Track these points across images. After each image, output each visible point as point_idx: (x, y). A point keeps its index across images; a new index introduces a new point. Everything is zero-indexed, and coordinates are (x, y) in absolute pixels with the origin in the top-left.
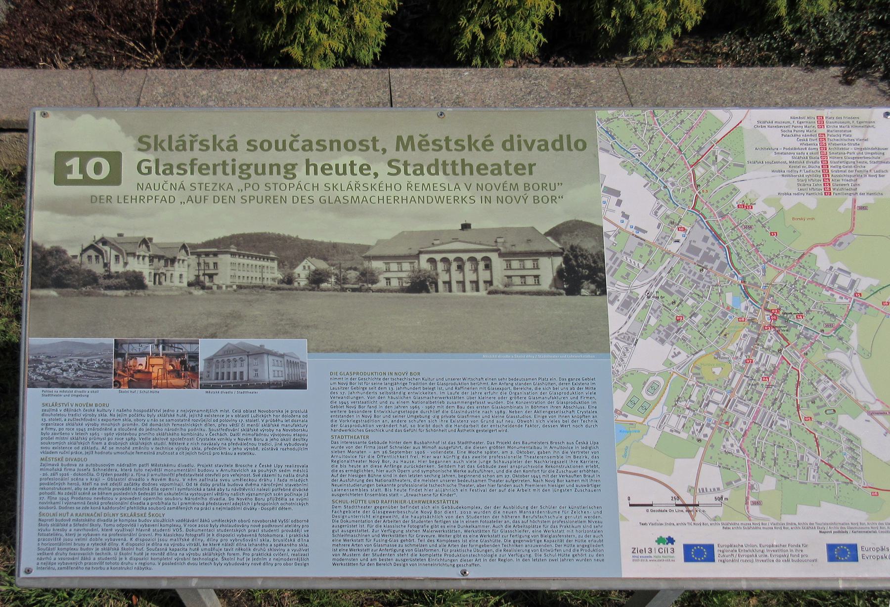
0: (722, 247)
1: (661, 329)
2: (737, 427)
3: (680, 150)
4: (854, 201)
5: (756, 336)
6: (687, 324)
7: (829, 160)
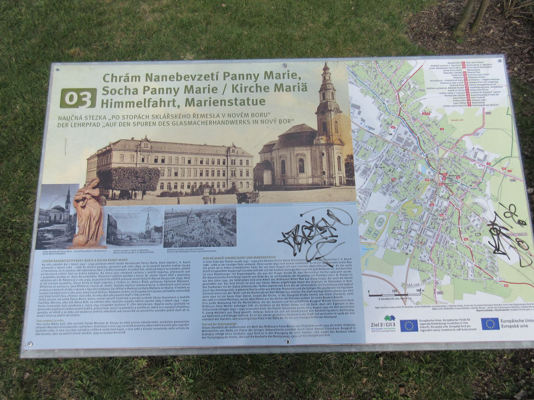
0: (415, 137)
1: (384, 186)
2: (427, 245)
3: (391, 82)
4: (484, 109)
5: (435, 189)
6: (398, 183)
7: (469, 86)
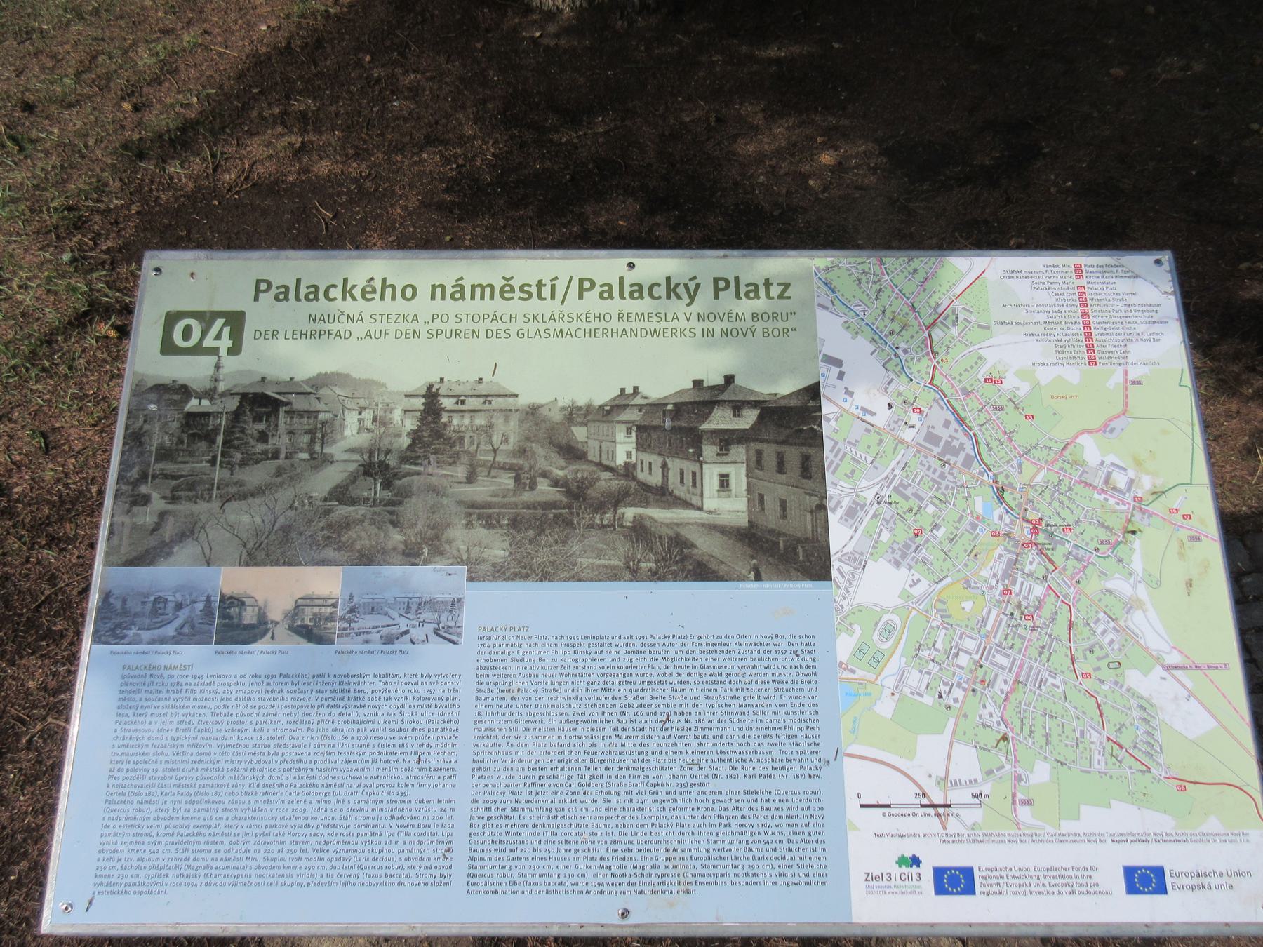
0: (967, 434)
1: (895, 546)
2: (997, 689)
3: (913, 308)
4: (1126, 373)
6: (927, 540)
7: (1092, 320)
